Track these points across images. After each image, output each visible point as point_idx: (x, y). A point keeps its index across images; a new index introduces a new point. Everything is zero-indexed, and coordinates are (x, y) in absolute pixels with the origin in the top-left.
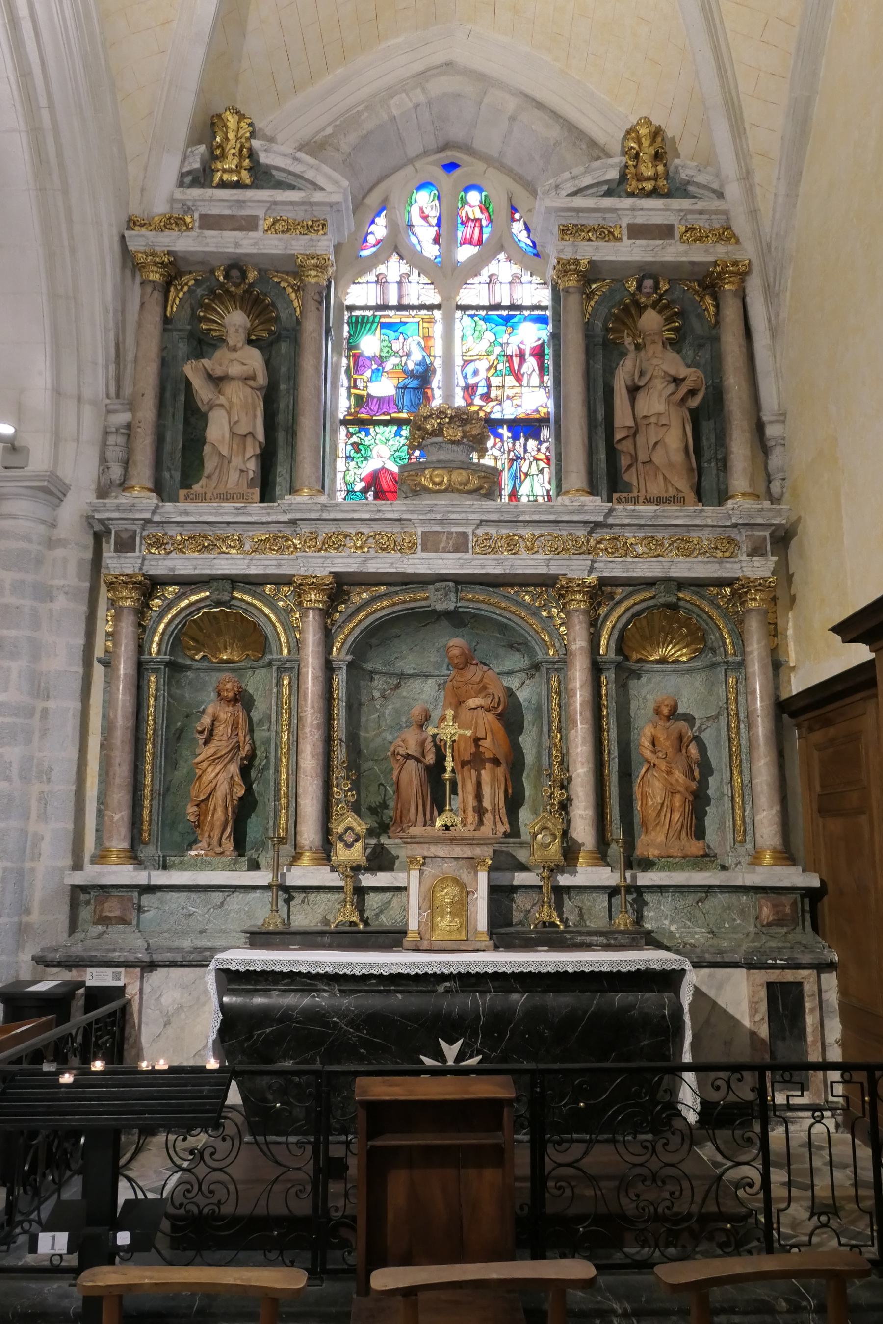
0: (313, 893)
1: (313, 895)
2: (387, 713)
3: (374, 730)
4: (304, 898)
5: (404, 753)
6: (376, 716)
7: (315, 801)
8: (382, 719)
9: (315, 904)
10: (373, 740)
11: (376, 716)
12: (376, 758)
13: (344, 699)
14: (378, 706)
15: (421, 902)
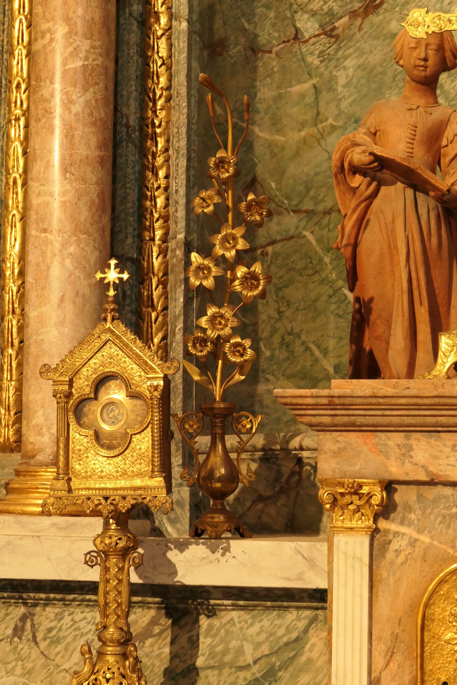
0: (48, 602)
1: (50, 611)
2: (342, 81)
3: (303, 125)
4: (23, 619)
5: (366, 159)
6: (307, 85)
7: (69, 308)
8: (325, 96)
9: (57, 641)
10: (298, 153)
11: (307, 85)
12: (308, 205)
13: (184, 11)
14: (313, 60)
15: (379, 661)
